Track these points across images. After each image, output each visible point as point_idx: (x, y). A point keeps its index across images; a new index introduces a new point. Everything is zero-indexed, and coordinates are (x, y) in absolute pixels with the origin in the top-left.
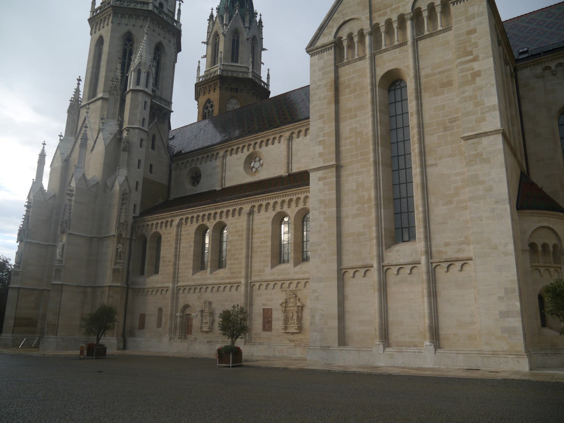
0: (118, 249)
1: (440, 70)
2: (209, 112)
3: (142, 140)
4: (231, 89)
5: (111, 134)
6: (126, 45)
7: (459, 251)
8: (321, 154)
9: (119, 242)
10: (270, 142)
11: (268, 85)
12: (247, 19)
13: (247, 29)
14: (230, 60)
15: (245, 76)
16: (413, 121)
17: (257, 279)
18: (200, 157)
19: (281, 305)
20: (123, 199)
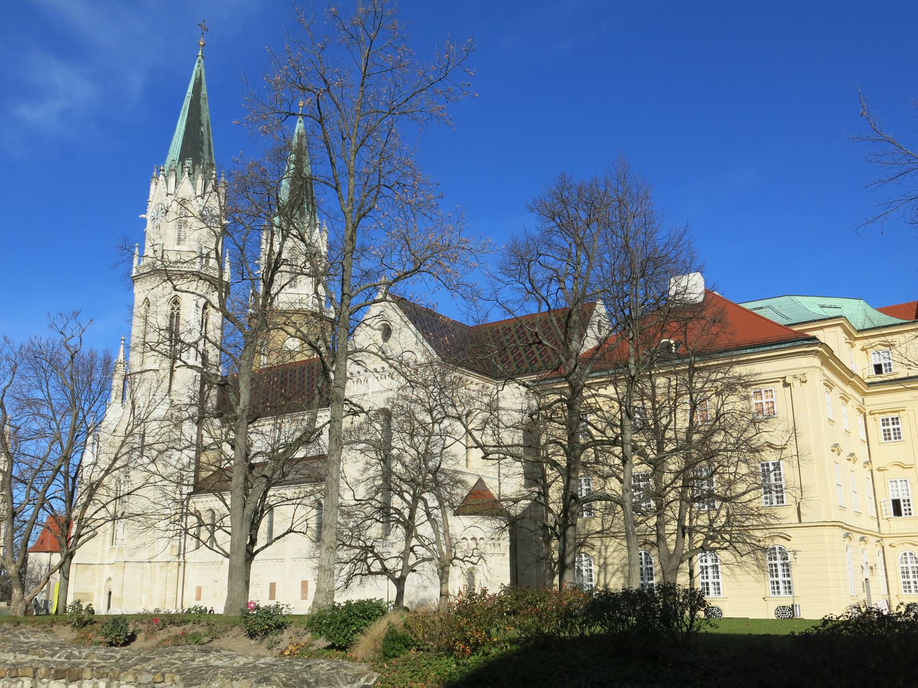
6: (173, 309)
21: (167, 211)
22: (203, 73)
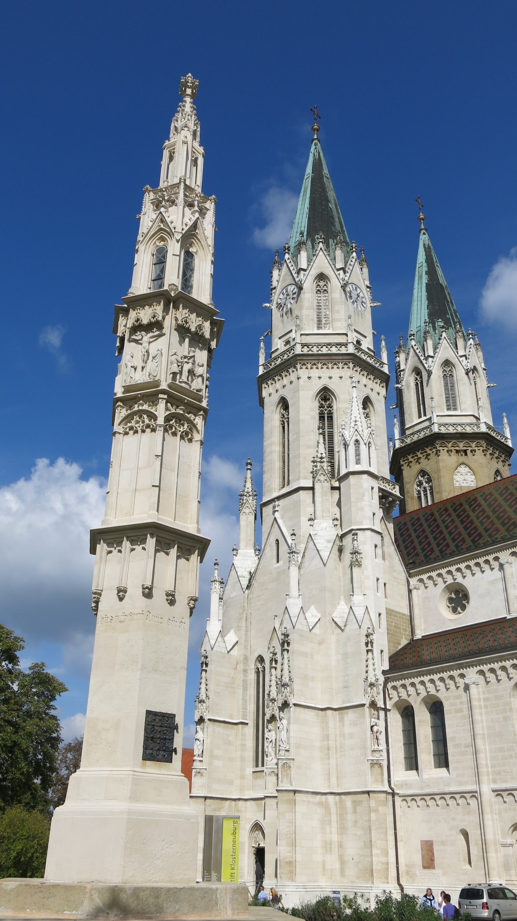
0: (372, 727)
2: (425, 490)
3: (376, 546)
4: (457, 452)
5: (328, 541)
6: (322, 406)
9: (371, 718)
12: (460, 343)
13: (464, 358)
14: (445, 408)
15: (476, 430)
20: (367, 644)
21: (300, 288)
22: (322, 154)
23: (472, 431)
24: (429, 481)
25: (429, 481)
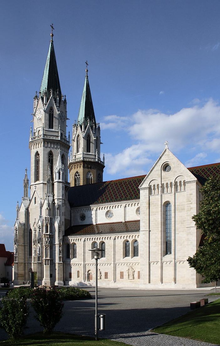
1: (182, 204)
3: (63, 203)
7: (183, 258)
8: (144, 226)
9: (60, 247)
10: (117, 207)
11: (103, 163)
16: (173, 220)
17: (118, 262)
18: (85, 209)
19: (127, 271)
23: (93, 161)
24: (79, 175)
25: (79, 175)
